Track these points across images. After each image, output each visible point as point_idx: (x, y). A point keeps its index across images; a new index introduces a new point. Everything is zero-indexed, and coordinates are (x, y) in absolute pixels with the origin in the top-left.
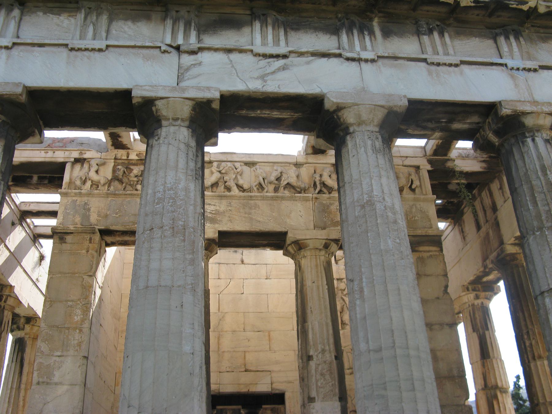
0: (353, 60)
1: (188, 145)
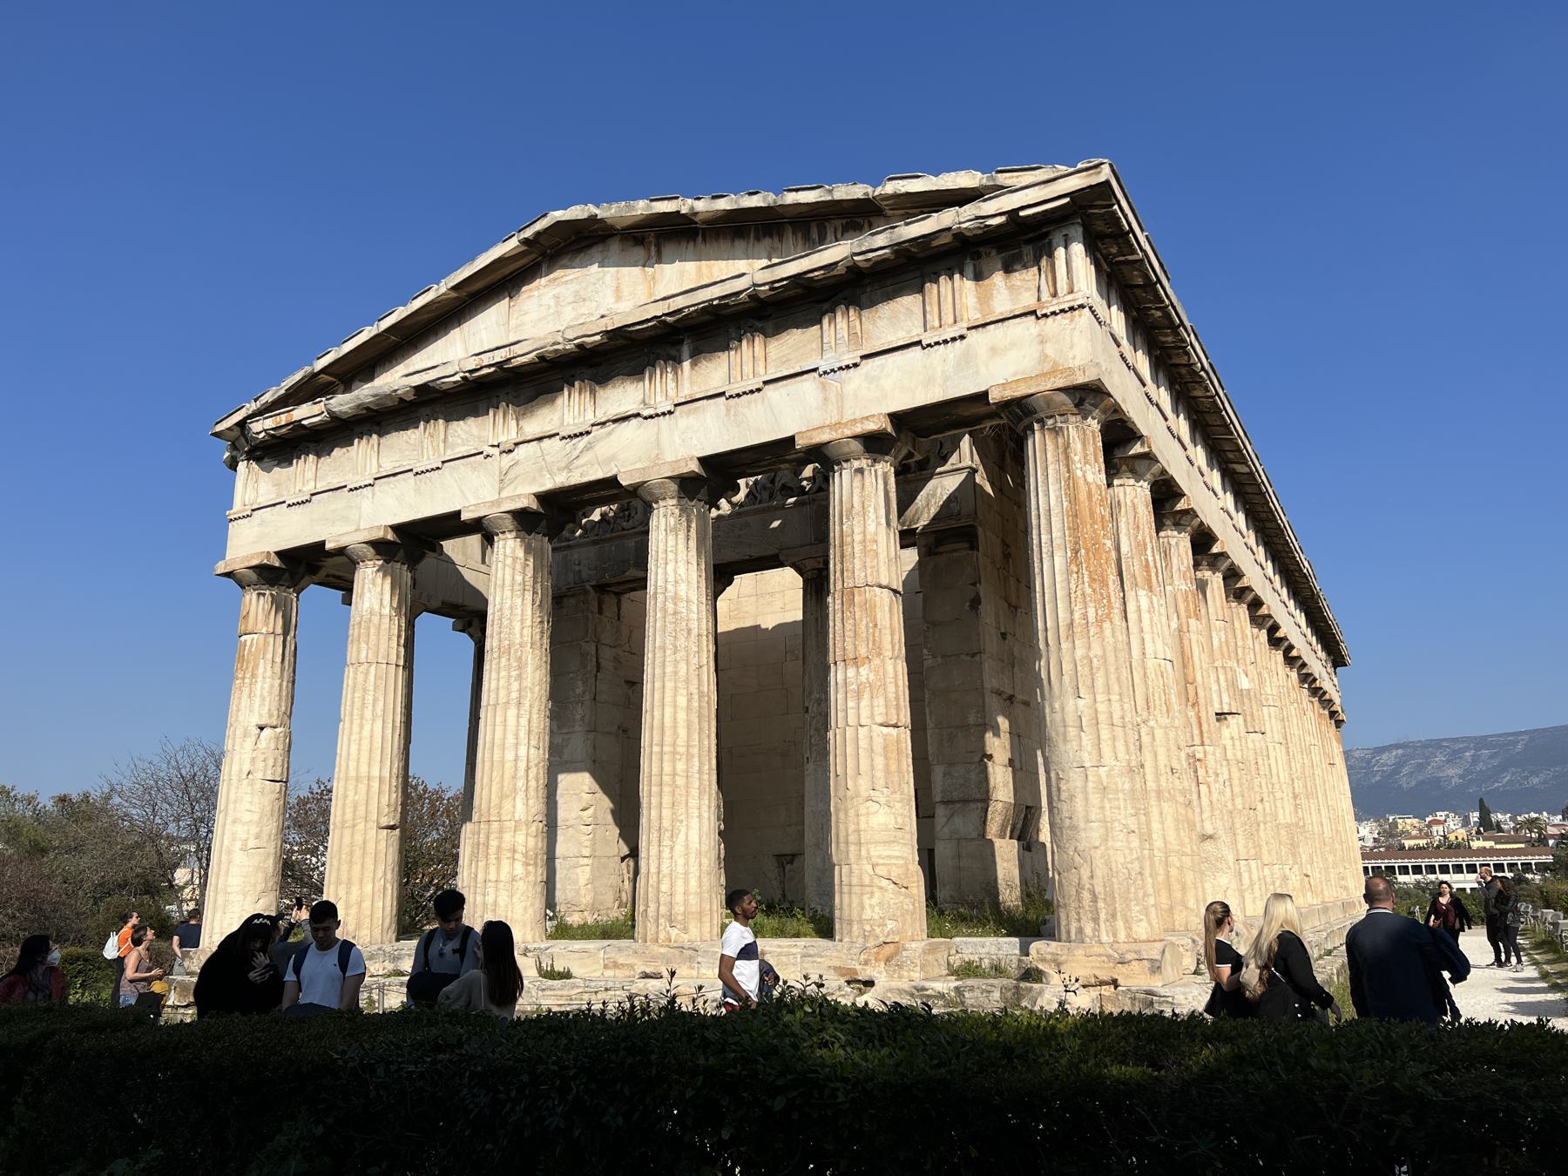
0: (651, 417)
1: (515, 559)
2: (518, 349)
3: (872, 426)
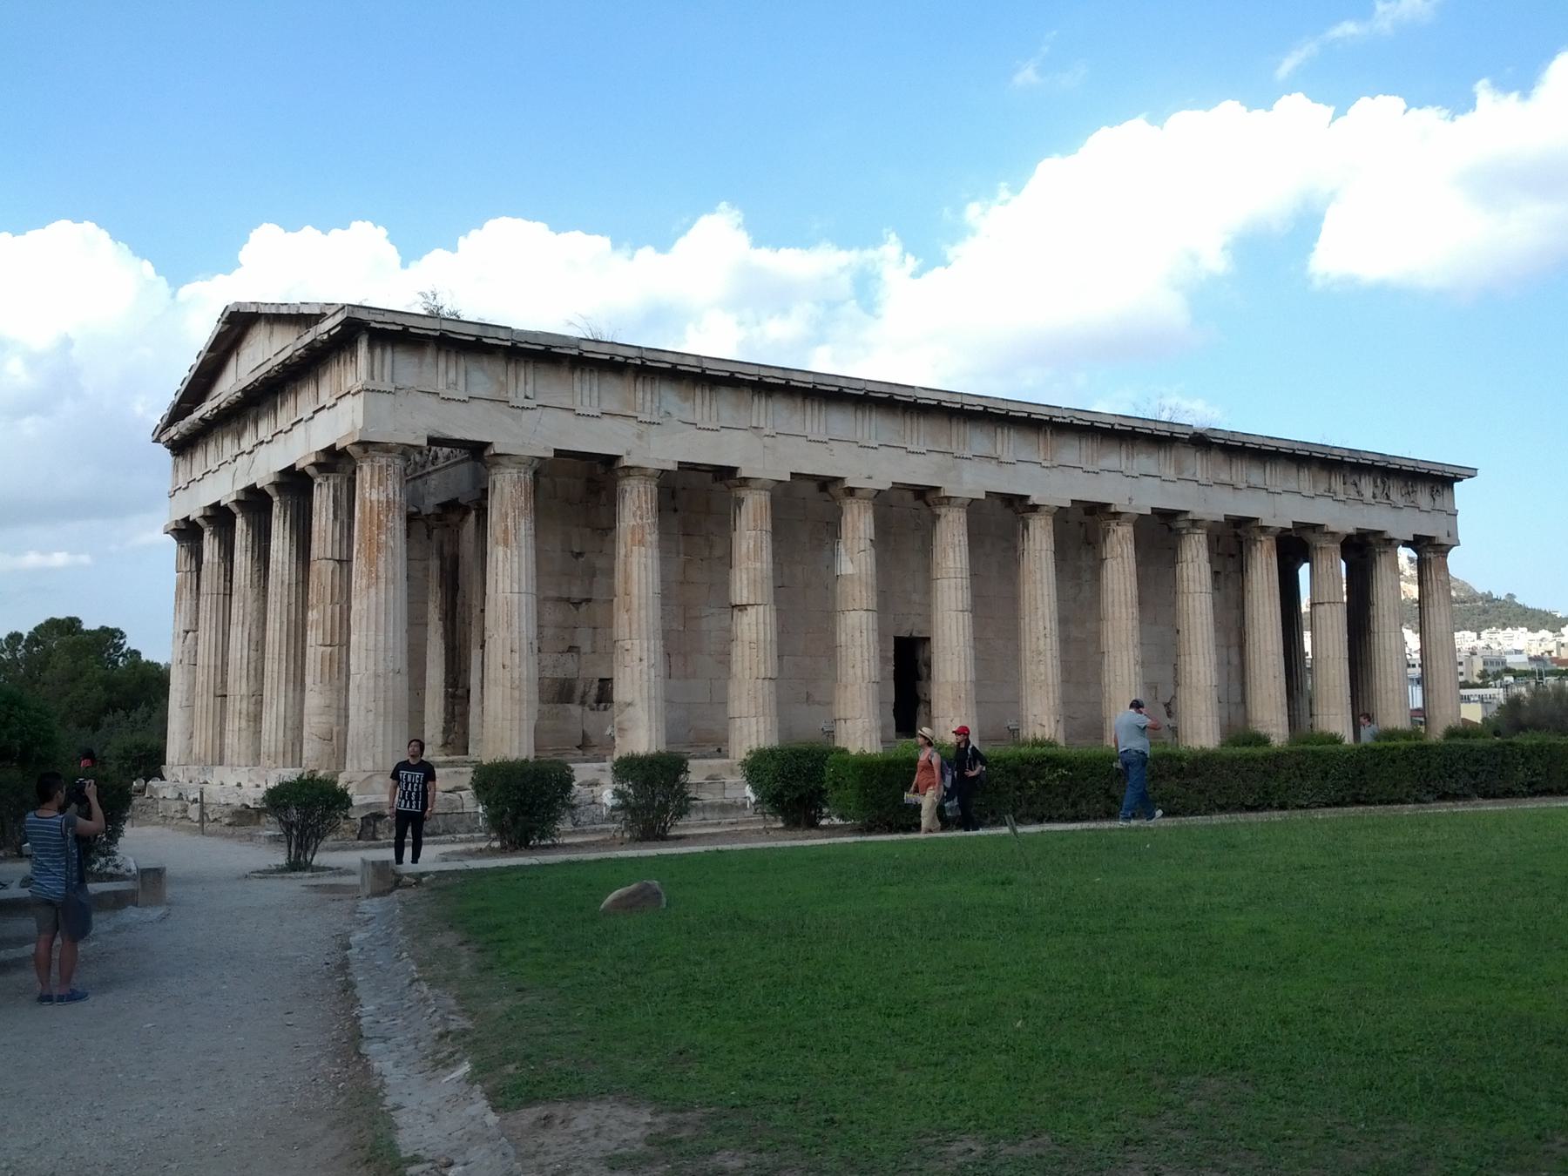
2: (222, 398)
3: (313, 459)
